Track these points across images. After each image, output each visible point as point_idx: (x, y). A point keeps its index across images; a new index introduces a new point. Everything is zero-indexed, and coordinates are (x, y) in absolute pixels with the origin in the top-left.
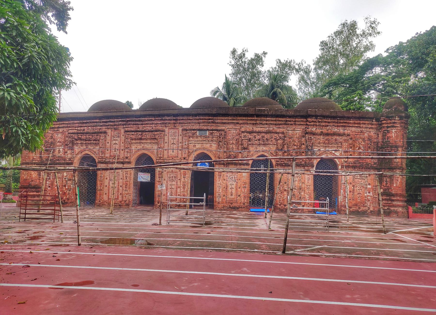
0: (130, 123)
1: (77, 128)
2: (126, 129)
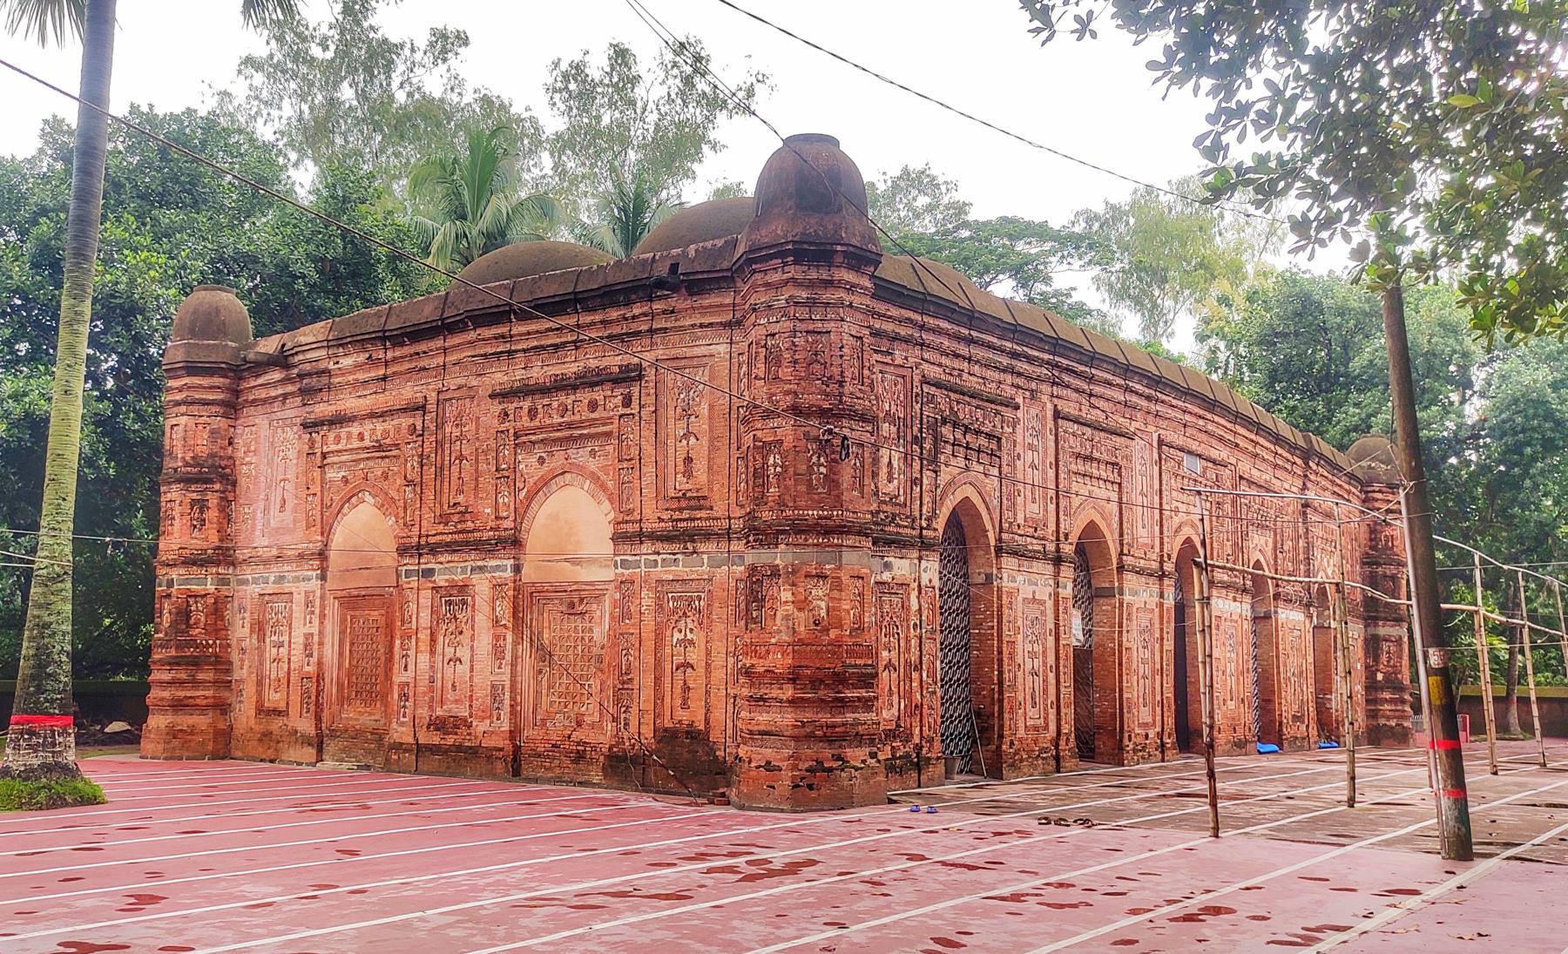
0: (1066, 378)
1: (944, 360)
2: (1061, 404)
